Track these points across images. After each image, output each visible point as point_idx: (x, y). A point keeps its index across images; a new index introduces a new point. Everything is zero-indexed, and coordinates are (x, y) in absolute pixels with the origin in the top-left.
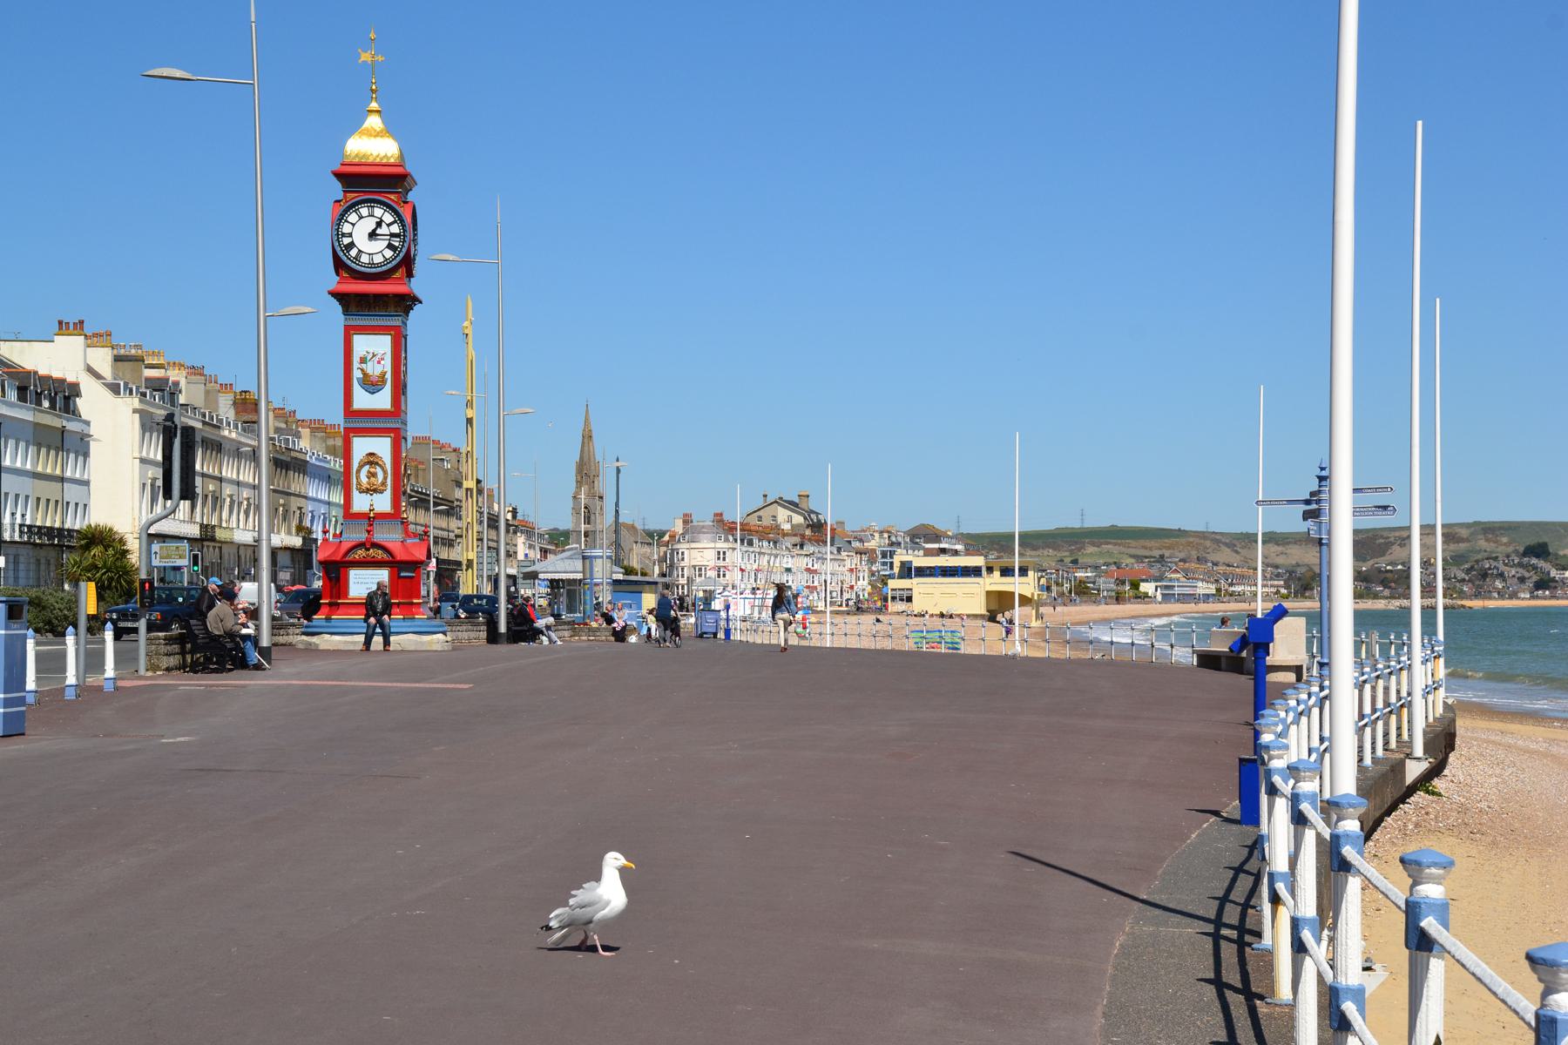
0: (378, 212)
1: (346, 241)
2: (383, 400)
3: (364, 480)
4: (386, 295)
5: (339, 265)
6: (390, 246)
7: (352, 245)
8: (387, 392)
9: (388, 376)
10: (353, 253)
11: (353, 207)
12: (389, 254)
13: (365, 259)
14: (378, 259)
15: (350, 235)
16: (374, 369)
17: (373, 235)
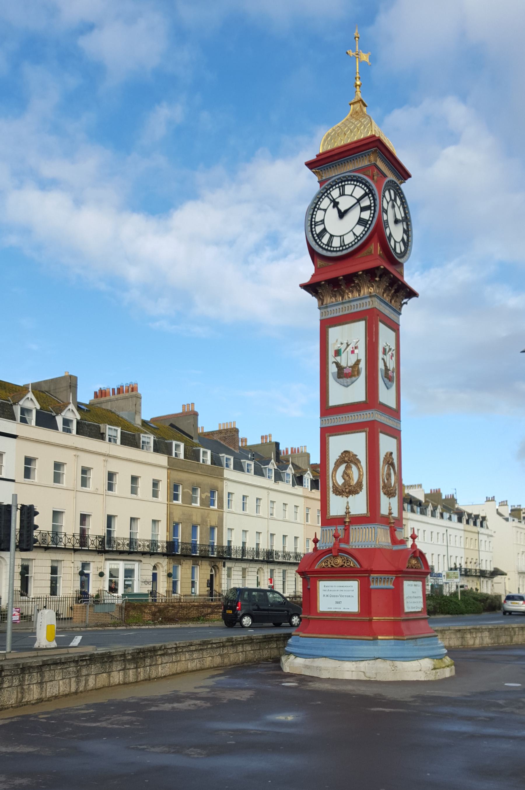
0: (348, 189)
1: (319, 229)
2: (356, 392)
3: (340, 481)
4: (355, 275)
5: (313, 253)
6: (361, 221)
7: (325, 230)
8: (360, 383)
9: (362, 365)
10: (325, 240)
11: (324, 193)
12: (359, 230)
13: (336, 243)
14: (349, 239)
15: (323, 222)
16: (347, 360)
17: (342, 215)
